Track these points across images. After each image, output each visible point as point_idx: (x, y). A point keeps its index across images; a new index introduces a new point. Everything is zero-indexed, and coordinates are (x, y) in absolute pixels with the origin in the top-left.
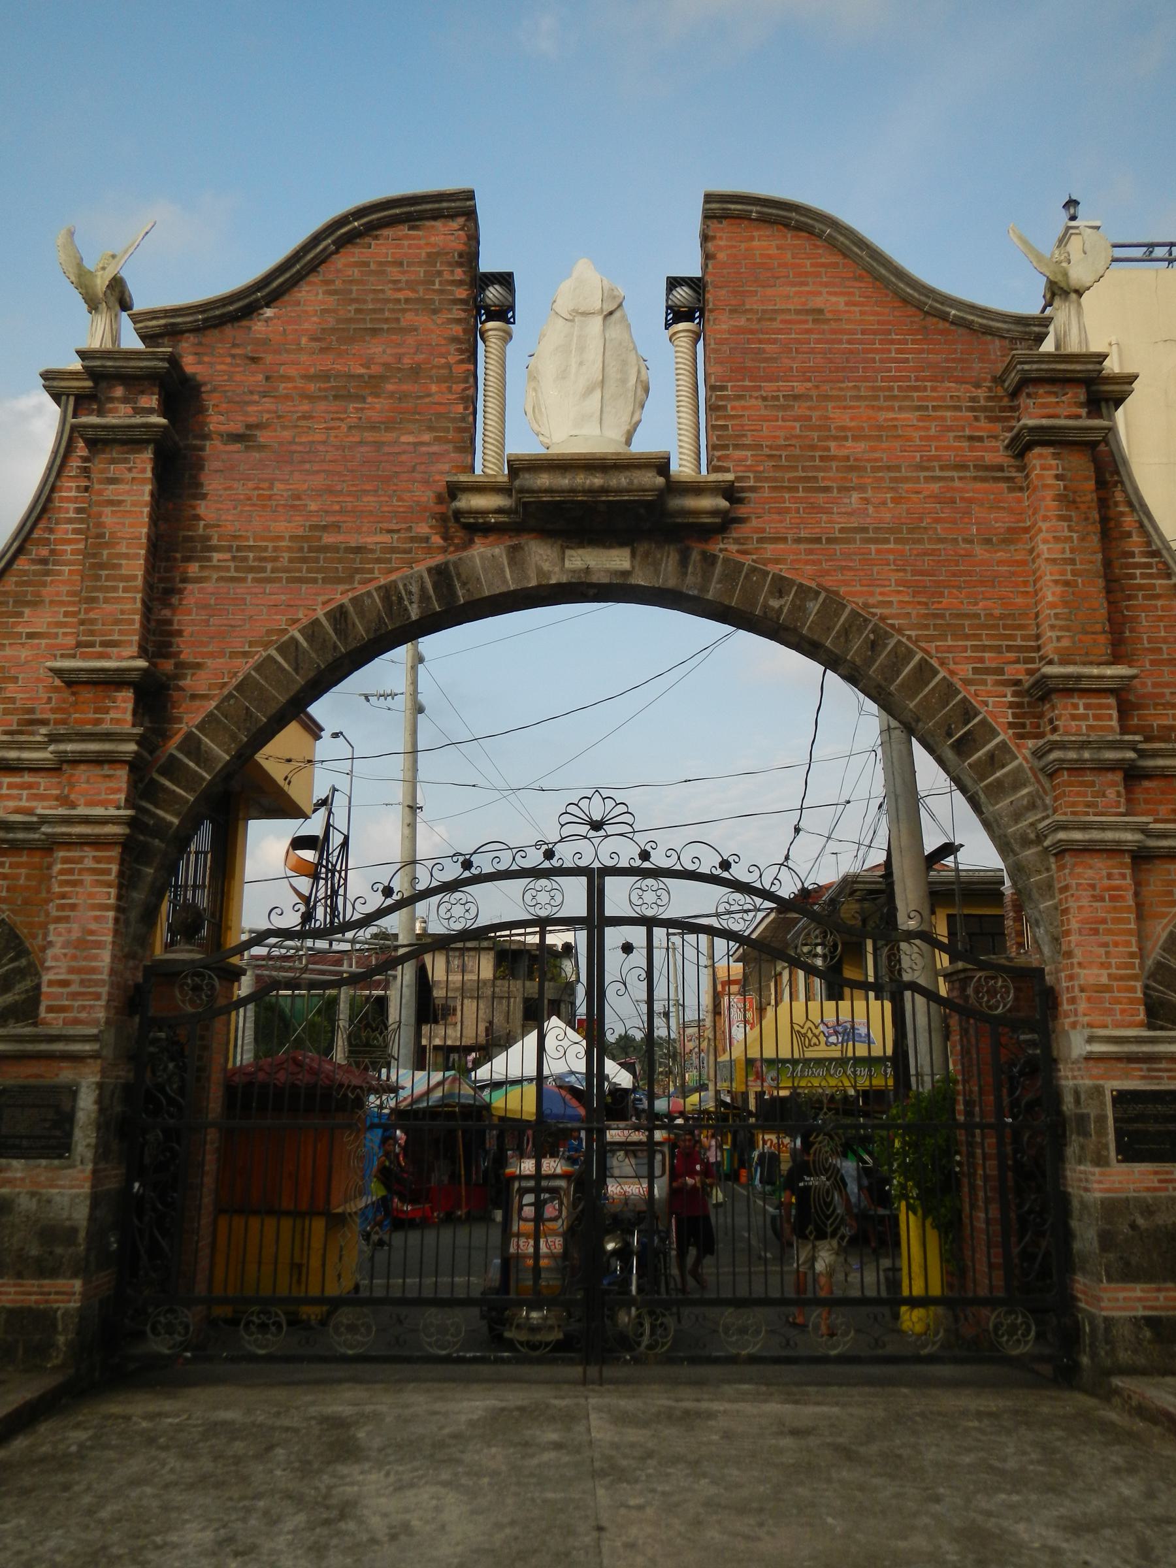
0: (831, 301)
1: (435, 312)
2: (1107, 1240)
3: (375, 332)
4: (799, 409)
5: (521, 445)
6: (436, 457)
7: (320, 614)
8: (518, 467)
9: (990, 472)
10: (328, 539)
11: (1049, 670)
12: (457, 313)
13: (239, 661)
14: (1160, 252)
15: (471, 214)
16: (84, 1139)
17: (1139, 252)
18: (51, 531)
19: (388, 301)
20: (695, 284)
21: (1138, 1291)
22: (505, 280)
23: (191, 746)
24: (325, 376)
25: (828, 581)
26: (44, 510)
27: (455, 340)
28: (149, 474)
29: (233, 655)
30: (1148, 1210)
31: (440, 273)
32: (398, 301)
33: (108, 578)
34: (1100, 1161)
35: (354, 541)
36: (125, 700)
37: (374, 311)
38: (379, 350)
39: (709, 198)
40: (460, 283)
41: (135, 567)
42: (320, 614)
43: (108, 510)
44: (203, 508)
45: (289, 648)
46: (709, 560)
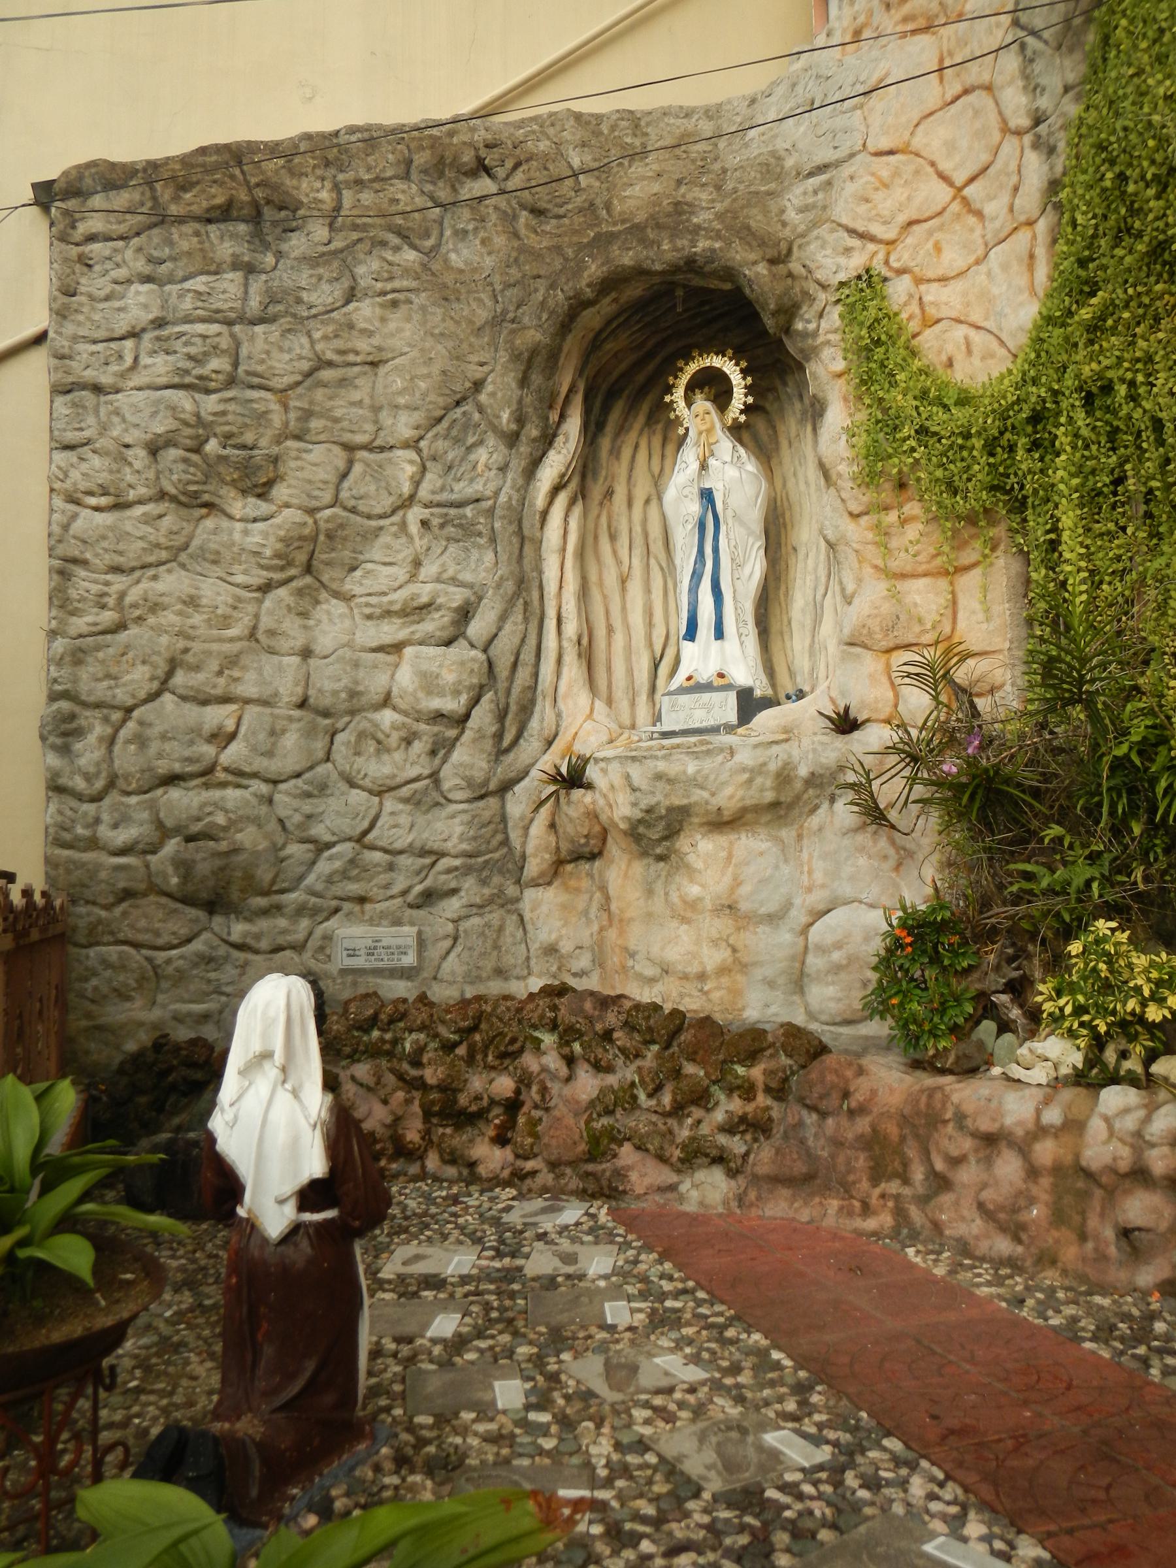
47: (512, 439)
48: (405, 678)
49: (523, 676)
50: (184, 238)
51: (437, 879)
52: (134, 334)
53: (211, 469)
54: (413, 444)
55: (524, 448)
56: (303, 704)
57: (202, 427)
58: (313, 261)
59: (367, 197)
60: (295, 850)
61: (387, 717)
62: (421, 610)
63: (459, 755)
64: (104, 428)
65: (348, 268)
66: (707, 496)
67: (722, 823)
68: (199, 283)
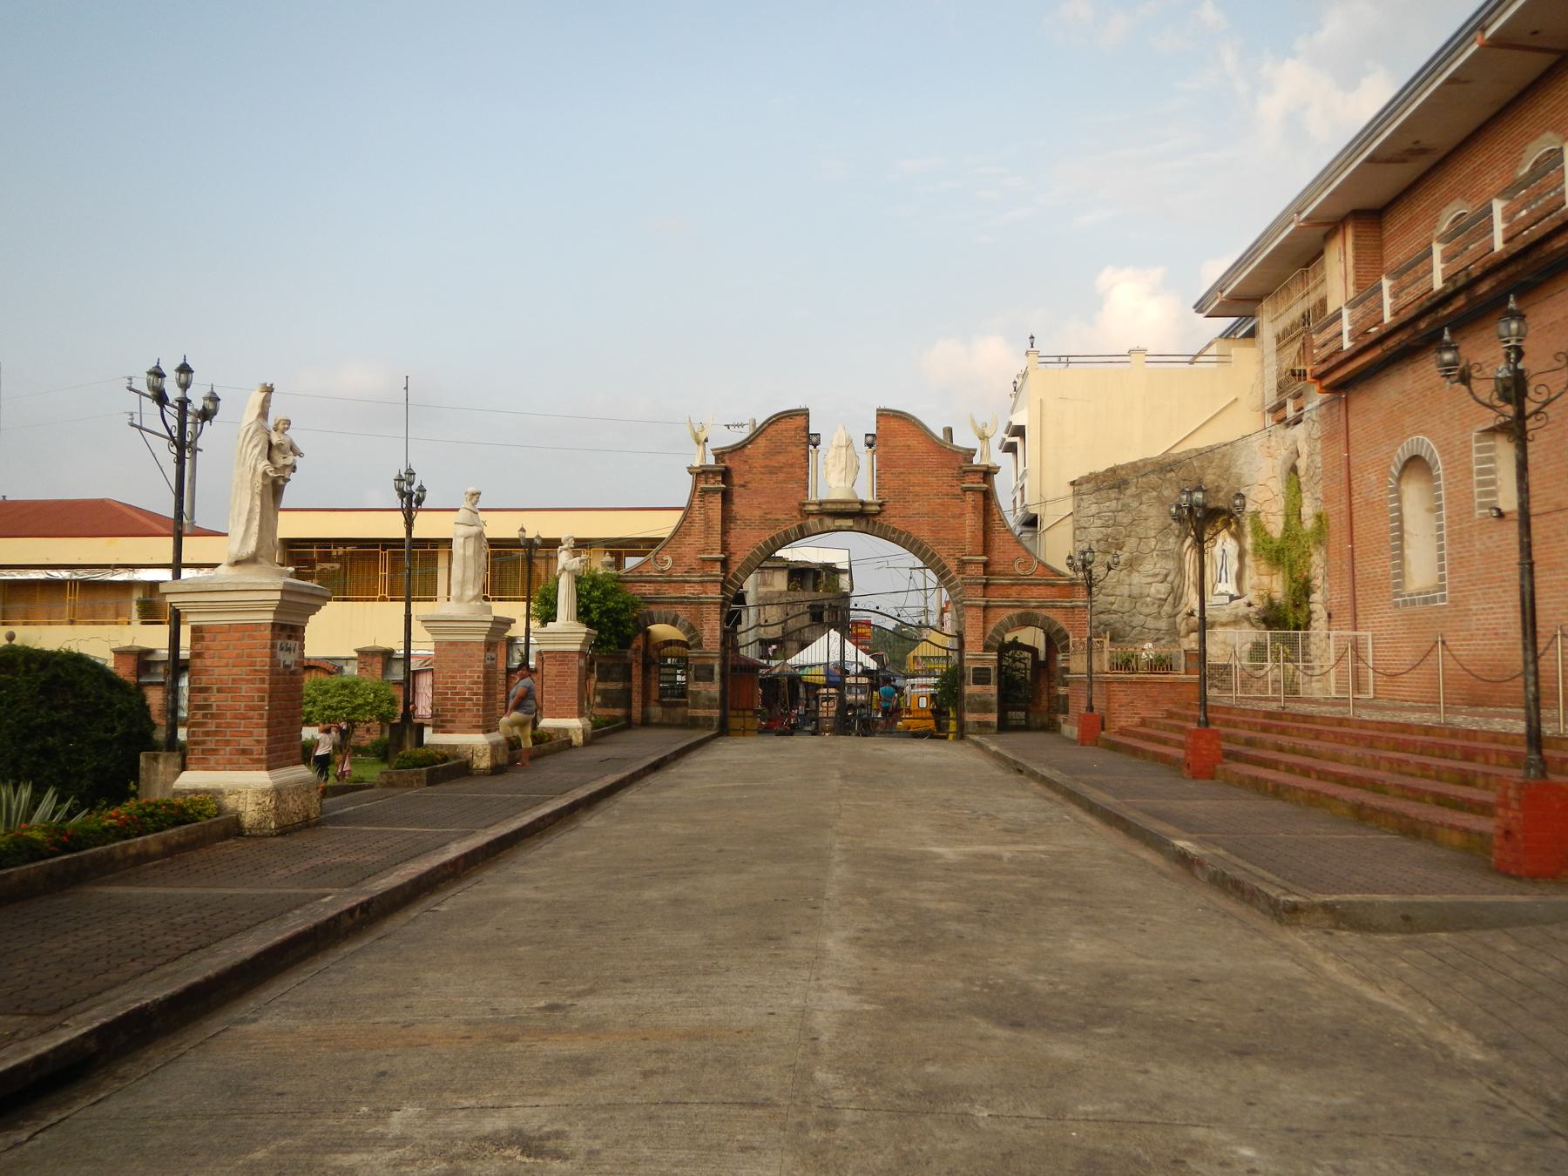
0: (913, 442)
2: (968, 704)
3: (780, 453)
4: (902, 477)
5: (823, 496)
6: (798, 492)
8: (820, 504)
9: (956, 496)
10: (769, 516)
11: (964, 558)
12: (803, 446)
14: (1064, 359)
15: (808, 415)
16: (717, 677)
17: (1056, 360)
20: (873, 435)
21: (975, 715)
23: (735, 576)
24: (766, 467)
25: (908, 529)
30: (979, 696)
34: (969, 685)
36: (718, 565)
38: (782, 459)
39: (878, 410)
41: (718, 528)
44: (734, 508)
45: (759, 548)
46: (875, 523)
47: (1178, 537)
48: (1153, 590)
49: (1180, 590)
50: (1104, 493)
51: (1160, 636)
52: (1093, 516)
53: (1110, 545)
54: (1155, 537)
55: (1181, 539)
56: (1129, 596)
57: (1108, 536)
58: (1132, 496)
59: (1144, 480)
60: (1128, 628)
61: (1148, 599)
62: (1155, 575)
63: (1165, 608)
64: (1087, 537)
65: (1140, 498)
66: (1224, 551)
67: (1223, 625)
68: (1107, 504)
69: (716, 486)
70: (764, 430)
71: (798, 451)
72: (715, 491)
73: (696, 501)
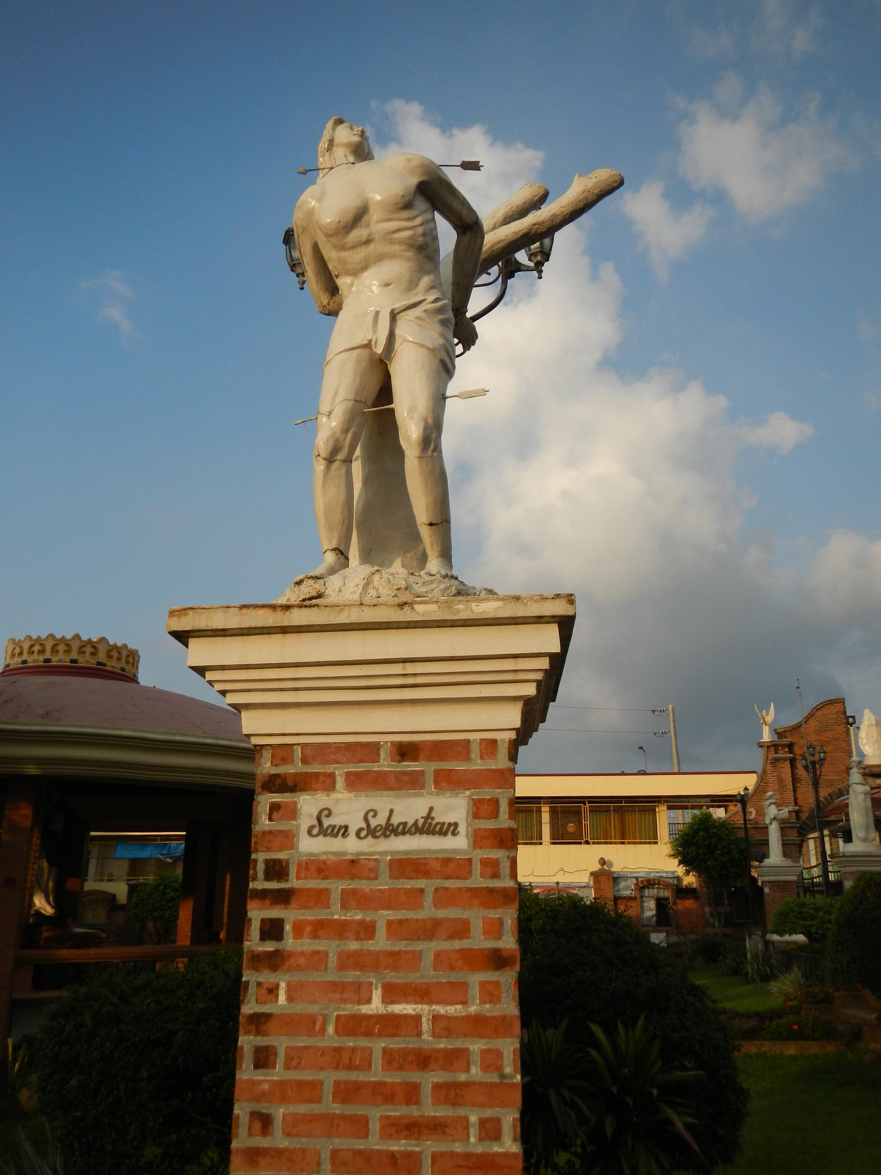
1: (840, 725)
3: (827, 730)
7: (826, 794)
13: (811, 804)
15: (844, 702)
18: (767, 776)
19: (829, 723)
22: (853, 717)
26: (765, 772)
27: (845, 732)
28: (789, 766)
29: (810, 803)
31: (839, 716)
32: (831, 723)
33: (786, 789)
35: (831, 778)
37: (826, 725)
38: (829, 734)
40: (844, 718)
41: (790, 786)
42: (826, 794)
43: (783, 774)
44: (798, 771)
69: (785, 755)
70: (813, 714)
71: (841, 729)
72: (785, 759)
73: (769, 767)
